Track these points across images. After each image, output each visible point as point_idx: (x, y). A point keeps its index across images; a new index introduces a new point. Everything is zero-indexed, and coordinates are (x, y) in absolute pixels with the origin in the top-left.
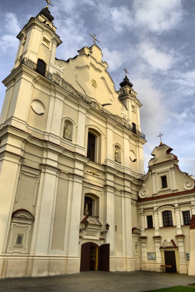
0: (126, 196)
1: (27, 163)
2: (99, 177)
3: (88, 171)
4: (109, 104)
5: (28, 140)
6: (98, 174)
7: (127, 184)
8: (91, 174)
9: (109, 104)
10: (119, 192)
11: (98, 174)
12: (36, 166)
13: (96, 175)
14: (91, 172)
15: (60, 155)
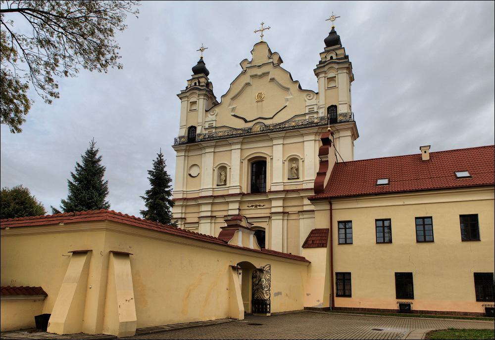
0: (305, 216)
1: (188, 221)
2: (264, 207)
3: (248, 207)
4: (286, 106)
5: (185, 204)
6: (262, 204)
7: (307, 202)
8: (254, 208)
9: (286, 106)
10: (297, 215)
11: (262, 204)
12: (196, 220)
13: (260, 206)
14: (252, 206)
15: (212, 204)
